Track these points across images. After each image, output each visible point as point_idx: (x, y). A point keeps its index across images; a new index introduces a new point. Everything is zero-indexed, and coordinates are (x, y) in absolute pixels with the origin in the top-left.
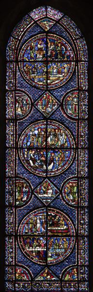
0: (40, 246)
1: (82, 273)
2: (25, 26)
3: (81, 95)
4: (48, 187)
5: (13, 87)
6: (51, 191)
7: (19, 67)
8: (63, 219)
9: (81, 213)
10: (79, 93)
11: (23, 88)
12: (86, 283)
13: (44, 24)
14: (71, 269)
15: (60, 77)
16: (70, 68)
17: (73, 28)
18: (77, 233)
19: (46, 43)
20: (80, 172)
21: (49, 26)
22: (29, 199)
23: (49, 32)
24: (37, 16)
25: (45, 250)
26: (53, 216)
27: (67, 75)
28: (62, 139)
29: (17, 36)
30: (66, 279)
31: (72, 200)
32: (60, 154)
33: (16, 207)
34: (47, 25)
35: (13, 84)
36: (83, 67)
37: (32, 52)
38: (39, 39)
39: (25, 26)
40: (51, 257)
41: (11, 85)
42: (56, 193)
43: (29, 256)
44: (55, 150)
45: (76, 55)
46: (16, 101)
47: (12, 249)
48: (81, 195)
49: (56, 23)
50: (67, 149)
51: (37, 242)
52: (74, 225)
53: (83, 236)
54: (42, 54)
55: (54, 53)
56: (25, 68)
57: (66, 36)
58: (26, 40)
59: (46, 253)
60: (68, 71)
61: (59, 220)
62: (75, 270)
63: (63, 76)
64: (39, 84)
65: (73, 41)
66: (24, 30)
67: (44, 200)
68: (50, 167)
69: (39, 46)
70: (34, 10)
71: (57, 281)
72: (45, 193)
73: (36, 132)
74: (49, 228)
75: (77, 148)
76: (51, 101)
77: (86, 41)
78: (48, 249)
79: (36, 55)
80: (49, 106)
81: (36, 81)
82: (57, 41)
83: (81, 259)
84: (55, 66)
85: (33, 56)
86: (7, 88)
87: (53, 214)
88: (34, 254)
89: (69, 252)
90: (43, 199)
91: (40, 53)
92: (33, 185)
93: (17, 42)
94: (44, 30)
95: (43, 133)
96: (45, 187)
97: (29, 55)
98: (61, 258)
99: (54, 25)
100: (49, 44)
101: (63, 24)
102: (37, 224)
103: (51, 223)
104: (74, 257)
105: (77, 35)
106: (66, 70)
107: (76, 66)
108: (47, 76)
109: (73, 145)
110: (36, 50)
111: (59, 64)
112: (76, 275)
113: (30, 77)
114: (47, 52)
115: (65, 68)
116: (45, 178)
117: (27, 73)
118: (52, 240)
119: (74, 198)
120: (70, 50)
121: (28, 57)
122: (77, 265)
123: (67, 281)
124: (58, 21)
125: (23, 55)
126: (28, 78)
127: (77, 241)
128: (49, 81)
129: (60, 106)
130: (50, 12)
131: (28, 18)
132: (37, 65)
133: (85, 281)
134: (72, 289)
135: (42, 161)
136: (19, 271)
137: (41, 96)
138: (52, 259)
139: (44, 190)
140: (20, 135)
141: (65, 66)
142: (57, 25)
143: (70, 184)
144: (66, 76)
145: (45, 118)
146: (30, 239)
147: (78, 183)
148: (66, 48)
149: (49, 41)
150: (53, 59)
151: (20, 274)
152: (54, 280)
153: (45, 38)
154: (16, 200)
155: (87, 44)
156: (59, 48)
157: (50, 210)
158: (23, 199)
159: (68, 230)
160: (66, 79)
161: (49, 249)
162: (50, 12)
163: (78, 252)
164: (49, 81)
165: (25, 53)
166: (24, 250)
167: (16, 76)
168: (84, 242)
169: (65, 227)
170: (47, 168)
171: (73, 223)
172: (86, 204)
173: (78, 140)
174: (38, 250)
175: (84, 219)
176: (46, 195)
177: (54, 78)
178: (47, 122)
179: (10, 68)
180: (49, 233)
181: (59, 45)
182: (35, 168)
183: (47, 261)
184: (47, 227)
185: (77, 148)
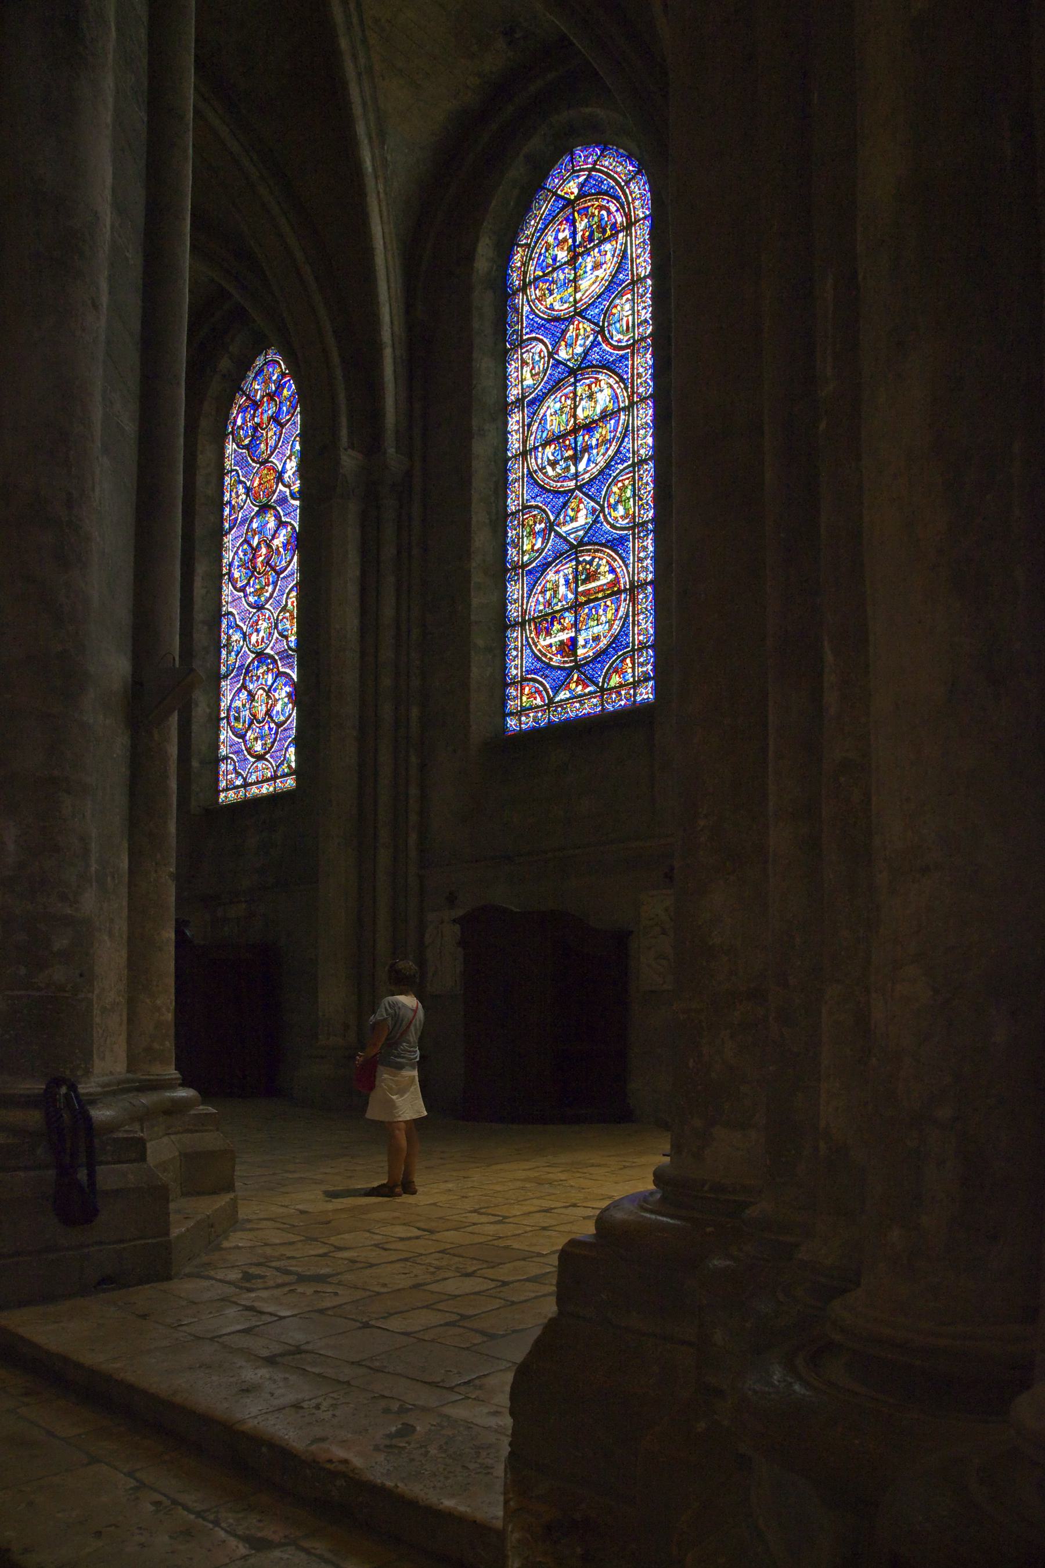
0: (562, 630)
1: (641, 665)
3: (638, 289)
4: (578, 506)
6: (583, 512)
8: (607, 562)
9: (639, 538)
10: (633, 290)
12: (651, 683)
14: (621, 662)
18: (632, 582)
20: (638, 451)
22: (546, 541)
25: (573, 634)
26: (588, 563)
28: (603, 399)
30: (612, 683)
31: (622, 517)
32: (600, 430)
33: (524, 566)
36: (642, 232)
40: (584, 647)
42: (594, 510)
43: (546, 656)
44: (589, 427)
46: (524, 363)
47: (516, 649)
48: (641, 499)
50: (614, 414)
51: (560, 623)
52: (627, 566)
53: (644, 585)
55: (587, 234)
59: (573, 641)
60: (613, 256)
61: (599, 566)
62: (628, 660)
67: (572, 536)
68: (582, 466)
71: (596, 692)
72: (573, 519)
73: (558, 405)
74: (580, 589)
75: (632, 404)
76: (582, 332)
78: (578, 631)
80: (579, 342)
83: (639, 634)
87: (588, 558)
88: (554, 648)
89: (617, 626)
90: (569, 534)
92: (553, 513)
95: (569, 402)
96: (573, 510)
98: (604, 642)
102: (558, 586)
103: (583, 577)
104: (627, 635)
106: (609, 256)
109: (624, 401)
112: (630, 671)
114: (574, 241)
116: (572, 491)
118: (586, 610)
119: (626, 510)
122: (633, 650)
123: (615, 687)
126: (543, 308)
127: (633, 600)
128: (578, 296)
129: (598, 332)
133: (647, 680)
134: (622, 703)
135: (566, 459)
136: (527, 689)
137: (564, 332)
138: (586, 650)
139: (572, 514)
140: (529, 425)
143: (620, 484)
145: (572, 372)
146: (545, 622)
147: (634, 477)
148: (608, 210)
151: (531, 695)
152: (590, 693)
154: (523, 552)
157: (582, 551)
158: (536, 548)
159: (617, 581)
161: (580, 630)
163: (634, 621)
166: (536, 646)
168: (647, 597)
169: (611, 577)
170: (576, 470)
171: (624, 562)
172: (651, 514)
173: (632, 388)
174: (561, 638)
175: (645, 548)
176: (574, 525)
178: (575, 377)
180: (582, 599)
182: (559, 478)
183: (575, 655)
184: (577, 587)
185: (632, 404)
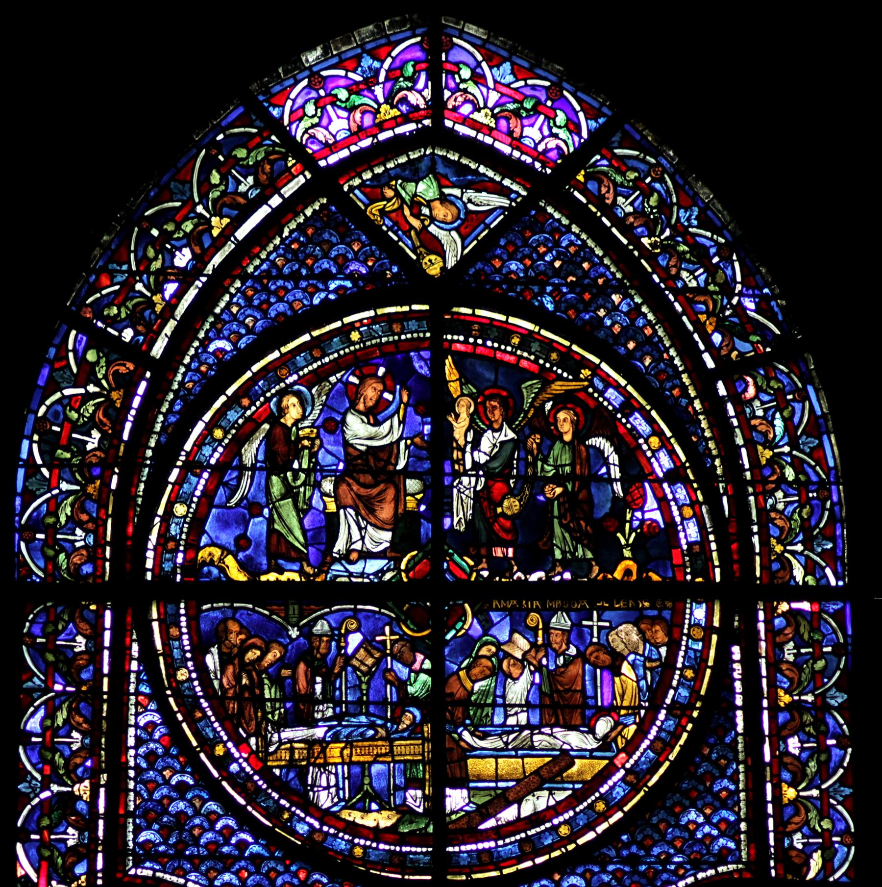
2: (218, 224)
5: (85, 852)
7: (148, 655)
11: (196, 862)
13: (415, 205)
15: (565, 758)
16: (669, 665)
17: (700, 255)
19: (434, 402)
21: (468, 222)
23: (461, 283)
24: (339, 125)
27: (641, 733)
29: (133, 321)
34: (440, 211)
35: (86, 824)
37: (290, 492)
38: (360, 363)
39: (218, 224)
41: (72, 837)
45: (731, 531)
49: (529, 202)
54: (386, 512)
56: (212, 660)
57: (631, 331)
58: (230, 367)
60: (655, 695)
63: (606, 743)
64: (354, 829)
65: (704, 381)
66: (200, 260)
69: (357, 428)
70: (312, 57)
77: (828, 389)
79: (331, 524)
81: (324, 800)
82: (546, 378)
84: (522, 643)
85: (297, 538)
86: (25, 867)
91: (366, 508)
93: (128, 384)
94: (415, 269)
97: (257, 527)
99: (513, 215)
100: (464, 409)
101: (609, 210)
105: (739, 327)
107: (727, 638)
108: (438, 738)
110: (324, 471)
111: (561, 621)
113: (260, 758)
114: (438, 499)
115: (618, 658)
117: (241, 710)
120: (674, 476)
121: (242, 542)
124: (551, 181)
125: (197, 525)
126: (240, 764)
128: (456, 799)
130: (478, 78)
131: (244, 141)
132: (338, 636)
141: (626, 635)
142: (541, 222)
144: (631, 746)
149: (465, 378)
150: (500, 566)
153: (417, 345)
155: (842, 419)
156: (561, 455)
160: (636, 778)
162: (478, 78)
164: (456, 799)
165: (208, 495)
167: (118, 746)
177: (507, 765)
179: (65, 664)
181: (565, 422)
